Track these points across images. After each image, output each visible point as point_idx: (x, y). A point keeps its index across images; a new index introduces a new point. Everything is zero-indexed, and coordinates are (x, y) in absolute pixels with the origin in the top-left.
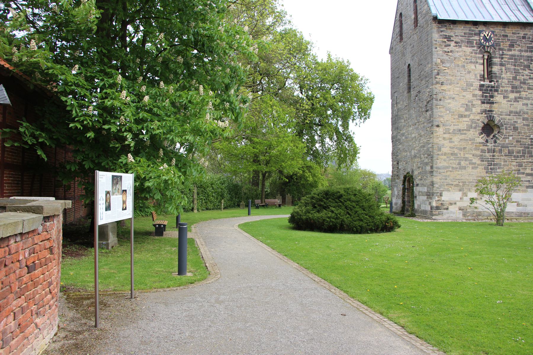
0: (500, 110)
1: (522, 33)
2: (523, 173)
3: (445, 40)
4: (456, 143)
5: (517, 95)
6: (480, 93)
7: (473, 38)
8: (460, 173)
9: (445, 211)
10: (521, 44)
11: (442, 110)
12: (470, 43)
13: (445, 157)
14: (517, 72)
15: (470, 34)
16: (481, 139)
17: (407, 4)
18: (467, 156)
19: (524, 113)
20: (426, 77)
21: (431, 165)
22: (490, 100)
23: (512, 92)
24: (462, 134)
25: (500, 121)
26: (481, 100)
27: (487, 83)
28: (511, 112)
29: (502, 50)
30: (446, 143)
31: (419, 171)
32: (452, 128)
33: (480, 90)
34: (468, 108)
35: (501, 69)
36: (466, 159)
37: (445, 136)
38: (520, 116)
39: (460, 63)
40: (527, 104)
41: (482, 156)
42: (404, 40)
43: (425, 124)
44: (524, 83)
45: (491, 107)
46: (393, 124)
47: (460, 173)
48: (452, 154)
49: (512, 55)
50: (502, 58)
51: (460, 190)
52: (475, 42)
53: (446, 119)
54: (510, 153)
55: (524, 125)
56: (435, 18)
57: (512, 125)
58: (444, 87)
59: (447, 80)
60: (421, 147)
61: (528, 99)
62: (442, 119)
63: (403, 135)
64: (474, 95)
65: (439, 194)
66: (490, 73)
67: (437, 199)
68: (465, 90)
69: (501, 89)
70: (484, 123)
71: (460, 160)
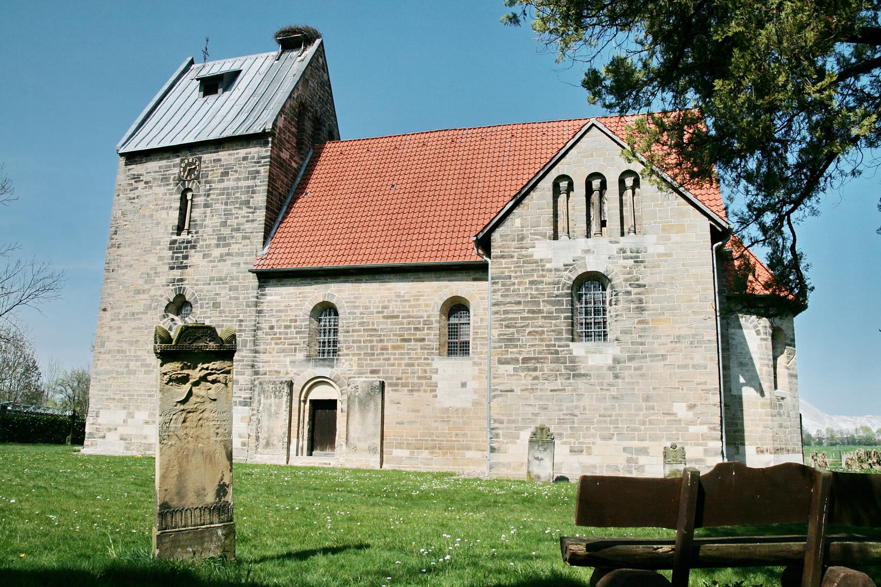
0: (196, 278)
1: (242, 152)
5: (224, 250)
7: (170, 172)
10: (239, 169)
11: (113, 285)
12: (165, 179)
13: (108, 356)
14: (228, 214)
18: (139, 353)
19: (232, 278)
22: (182, 263)
23: (218, 246)
24: (135, 319)
25: (193, 294)
26: (169, 264)
28: (212, 279)
32: (123, 312)
33: (170, 249)
34: (149, 279)
35: (205, 213)
36: (137, 358)
37: (113, 324)
38: (226, 283)
39: (147, 213)
40: (239, 264)
44: (238, 230)
47: (126, 380)
48: (118, 351)
49: (224, 189)
50: (208, 195)
52: (172, 177)
55: (230, 298)
58: (120, 251)
61: (242, 254)
62: (111, 299)
64: (161, 258)
69: (201, 243)
70: (169, 300)
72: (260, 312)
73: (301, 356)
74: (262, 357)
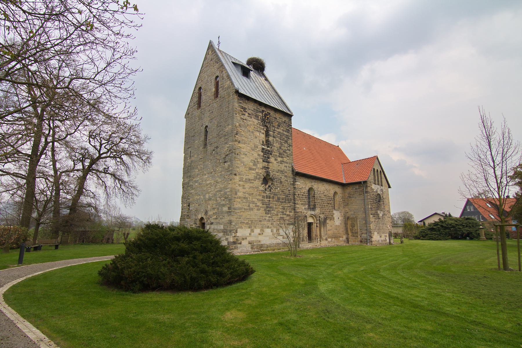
2: (285, 214)
3: (242, 110)
4: (247, 189)
5: (282, 159)
6: (262, 154)
8: (249, 213)
9: (239, 245)
11: (239, 162)
12: (257, 117)
15: (257, 110)
16: (262, 188)
17: (208, 80)
18: (254, 200)
20: (225, 135)
21: (229, 206)
23: (279, 157)
24: (251, 183)
27: (265, 147)
28: (279, 170)
29: (274, 127)
30: (240, 188)
31: (214, 212)
32: (245, 177)
33: (262, 152)
36: (253, 202)
41: (262, 200)
42: (202, 108)
43: (223, 173)
44: (285, 152)
45: (268, 165)
46: (185, 173)
47: (249, 213)
48: (244, 198)
50: (274, 133)
51: (249, 228)
53: (241, 170)
54: (279, 199)
56: (237, 92)
57: (279, 179)
58: (240, 145)
59: (243, 140)
60: (217, 191)
61: (287, 163)
62: (238, 169)
63: (196, 182)
64: (259, 155)
65: (235, 231)
66: (267, 141)
67: (234, 235)
68: (253, 150)
71: (249, 203)
72: (295, 188)
73: (307, 206)
74: (297, 206)
